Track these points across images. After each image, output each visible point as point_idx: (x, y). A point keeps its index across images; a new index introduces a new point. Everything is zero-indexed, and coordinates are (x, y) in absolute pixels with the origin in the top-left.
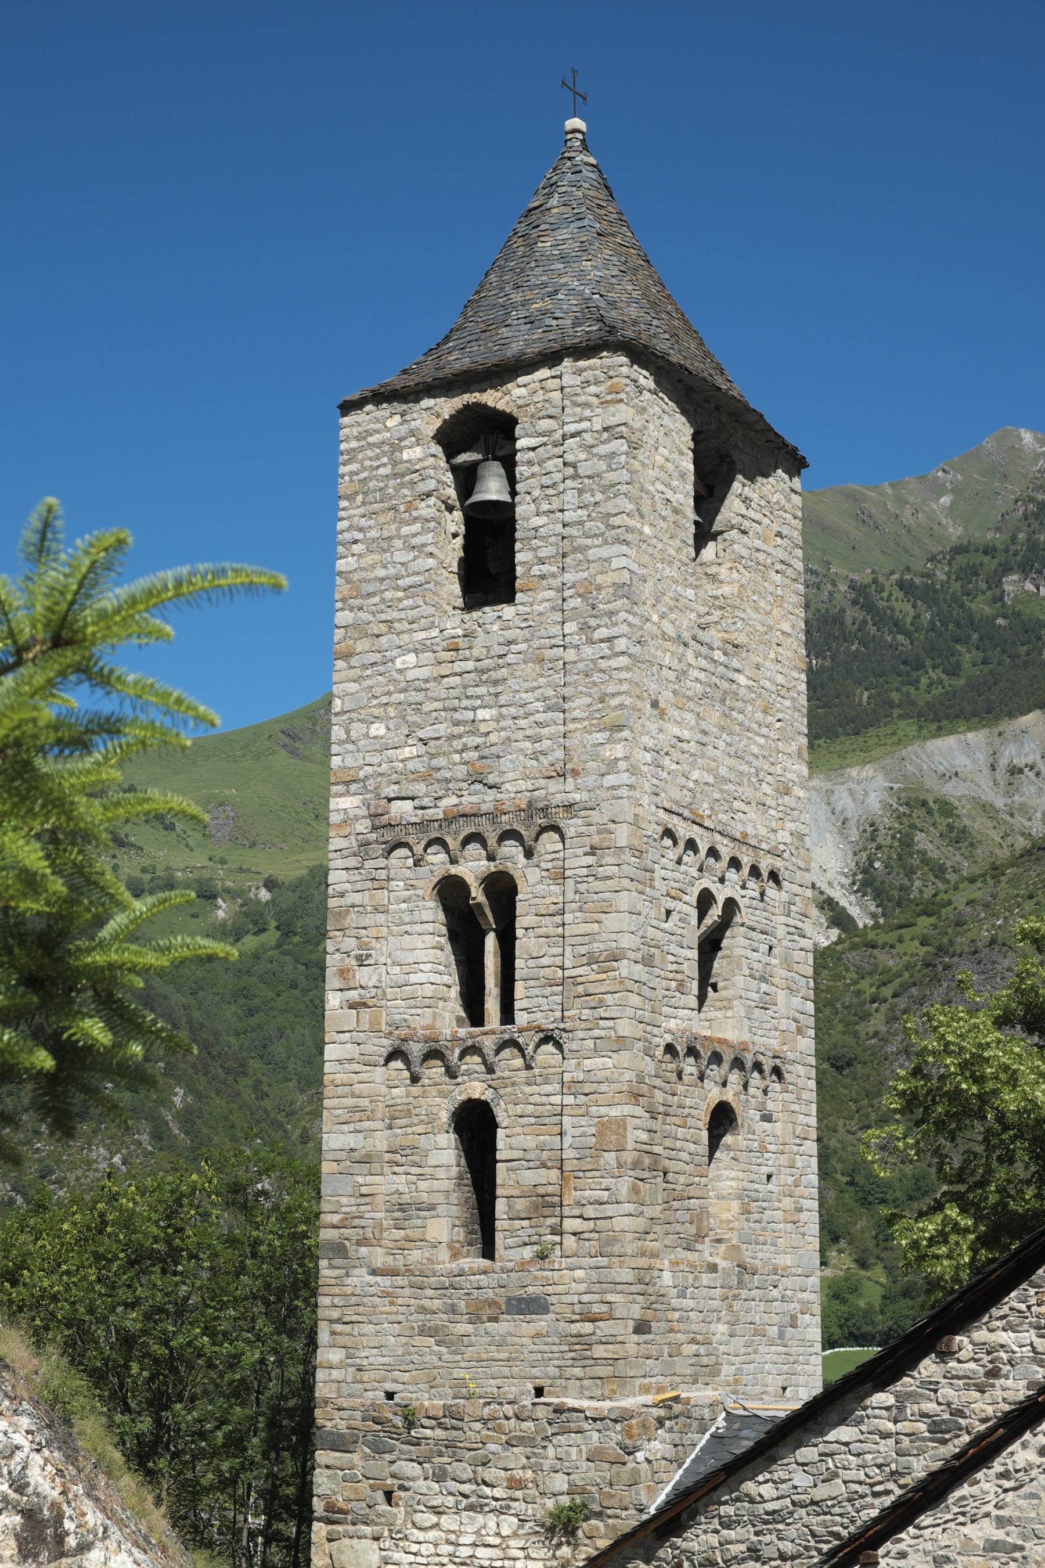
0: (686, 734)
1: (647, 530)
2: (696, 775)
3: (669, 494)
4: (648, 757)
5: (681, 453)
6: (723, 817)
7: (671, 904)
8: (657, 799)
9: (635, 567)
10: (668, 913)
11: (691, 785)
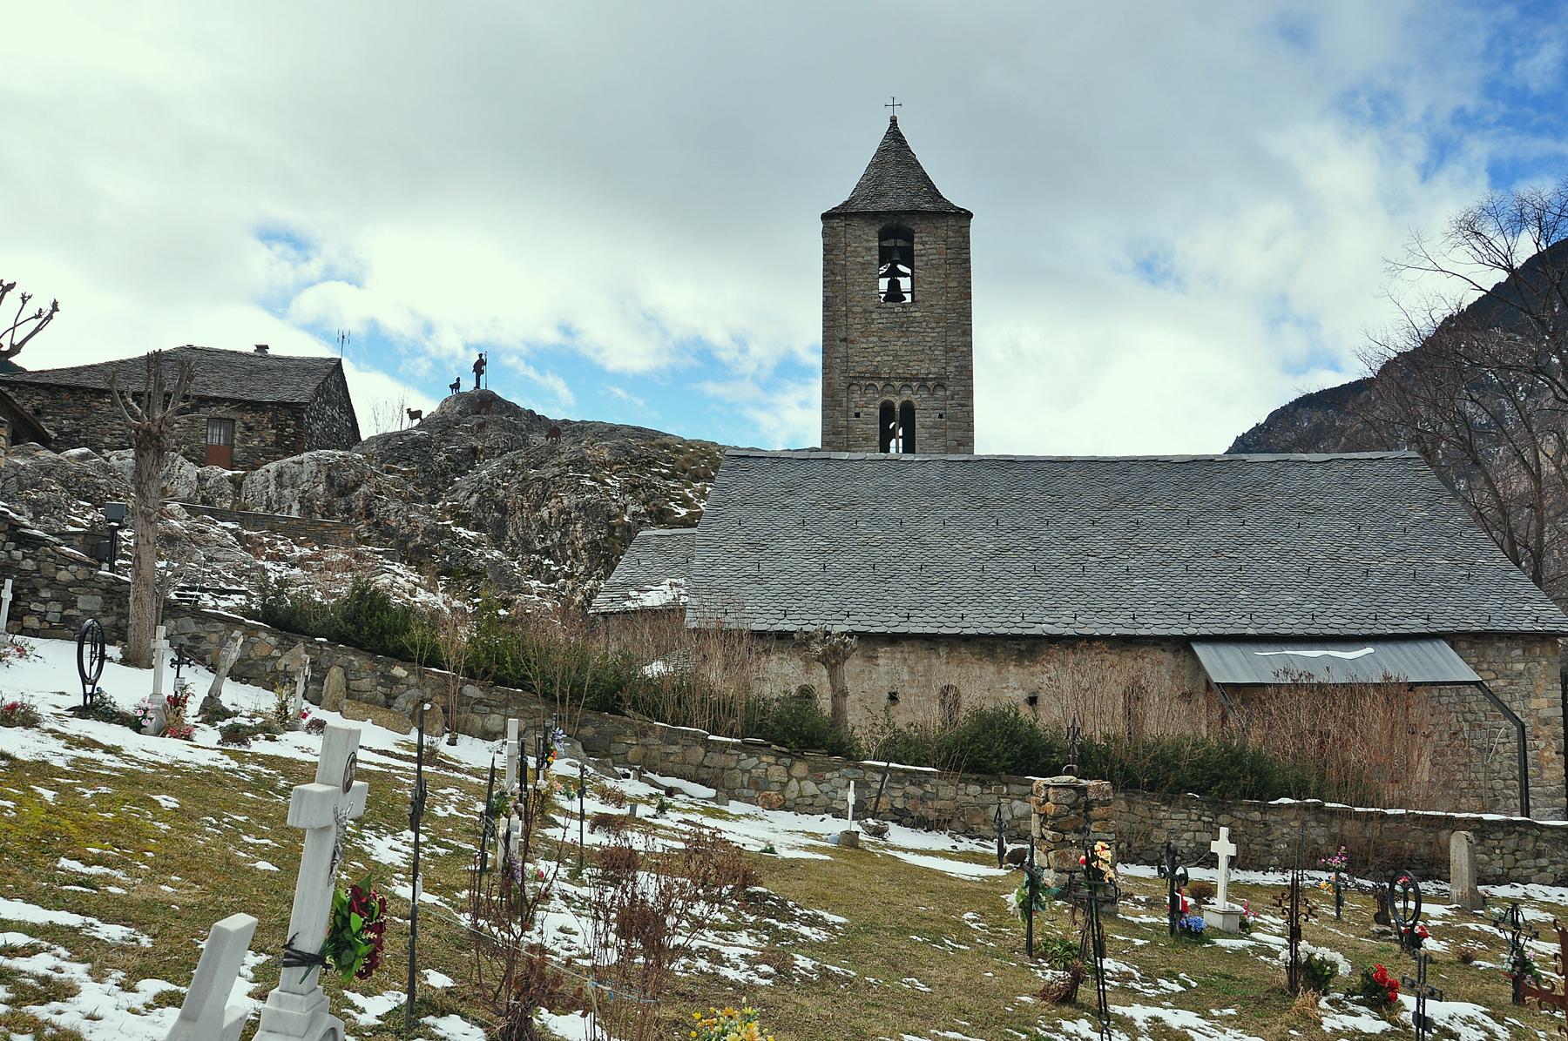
0: (871, 345)
1: (838, 278)
2: (879, 359)
3: (860, 259)
4: (838, 360)
5: (868, 241)
6: (901, 371)
7: (857, 410)
8: (846, 375)
9: (830, 294)
10: (857, 415)
11: (875, 363)
